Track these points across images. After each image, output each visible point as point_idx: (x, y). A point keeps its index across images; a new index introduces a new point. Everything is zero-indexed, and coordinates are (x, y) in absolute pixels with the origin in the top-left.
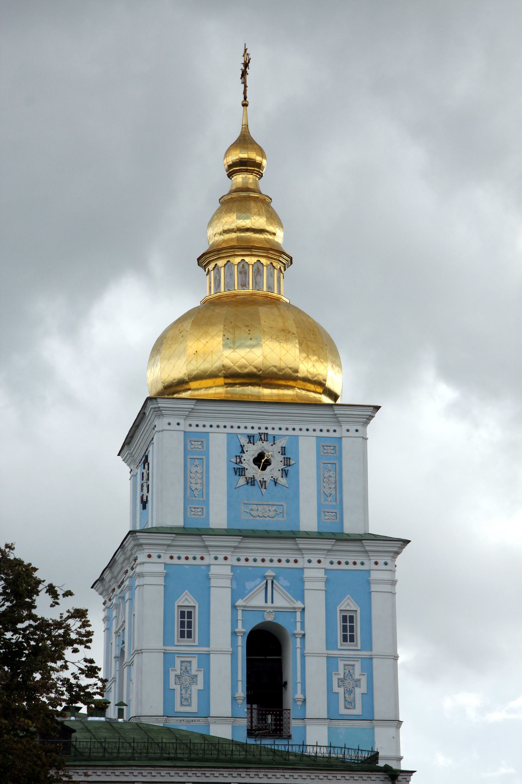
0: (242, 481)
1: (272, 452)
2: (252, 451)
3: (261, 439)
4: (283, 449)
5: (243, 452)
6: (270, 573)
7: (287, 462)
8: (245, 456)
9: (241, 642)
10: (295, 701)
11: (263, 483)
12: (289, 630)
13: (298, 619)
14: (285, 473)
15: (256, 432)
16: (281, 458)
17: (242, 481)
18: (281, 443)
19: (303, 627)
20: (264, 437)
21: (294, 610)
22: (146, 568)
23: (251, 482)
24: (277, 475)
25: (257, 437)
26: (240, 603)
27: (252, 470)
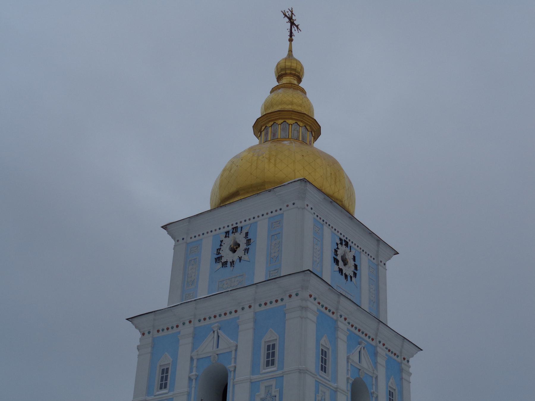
0: (336, 268)
1: (349, 257)
3: (345, 245)
4: (354, 257)
5: (338, 248)
7: (356, 266)
8: (339, 252)
11: (346, 276)
13: (374, 382)
14: (355, 274)
15: (342, 237)
16: (353, 263)
17: (336, 268)
20: (347, 244)
23: (341, 270)
24: (352, 275)
25: (344, 243)
27: (341, 263)
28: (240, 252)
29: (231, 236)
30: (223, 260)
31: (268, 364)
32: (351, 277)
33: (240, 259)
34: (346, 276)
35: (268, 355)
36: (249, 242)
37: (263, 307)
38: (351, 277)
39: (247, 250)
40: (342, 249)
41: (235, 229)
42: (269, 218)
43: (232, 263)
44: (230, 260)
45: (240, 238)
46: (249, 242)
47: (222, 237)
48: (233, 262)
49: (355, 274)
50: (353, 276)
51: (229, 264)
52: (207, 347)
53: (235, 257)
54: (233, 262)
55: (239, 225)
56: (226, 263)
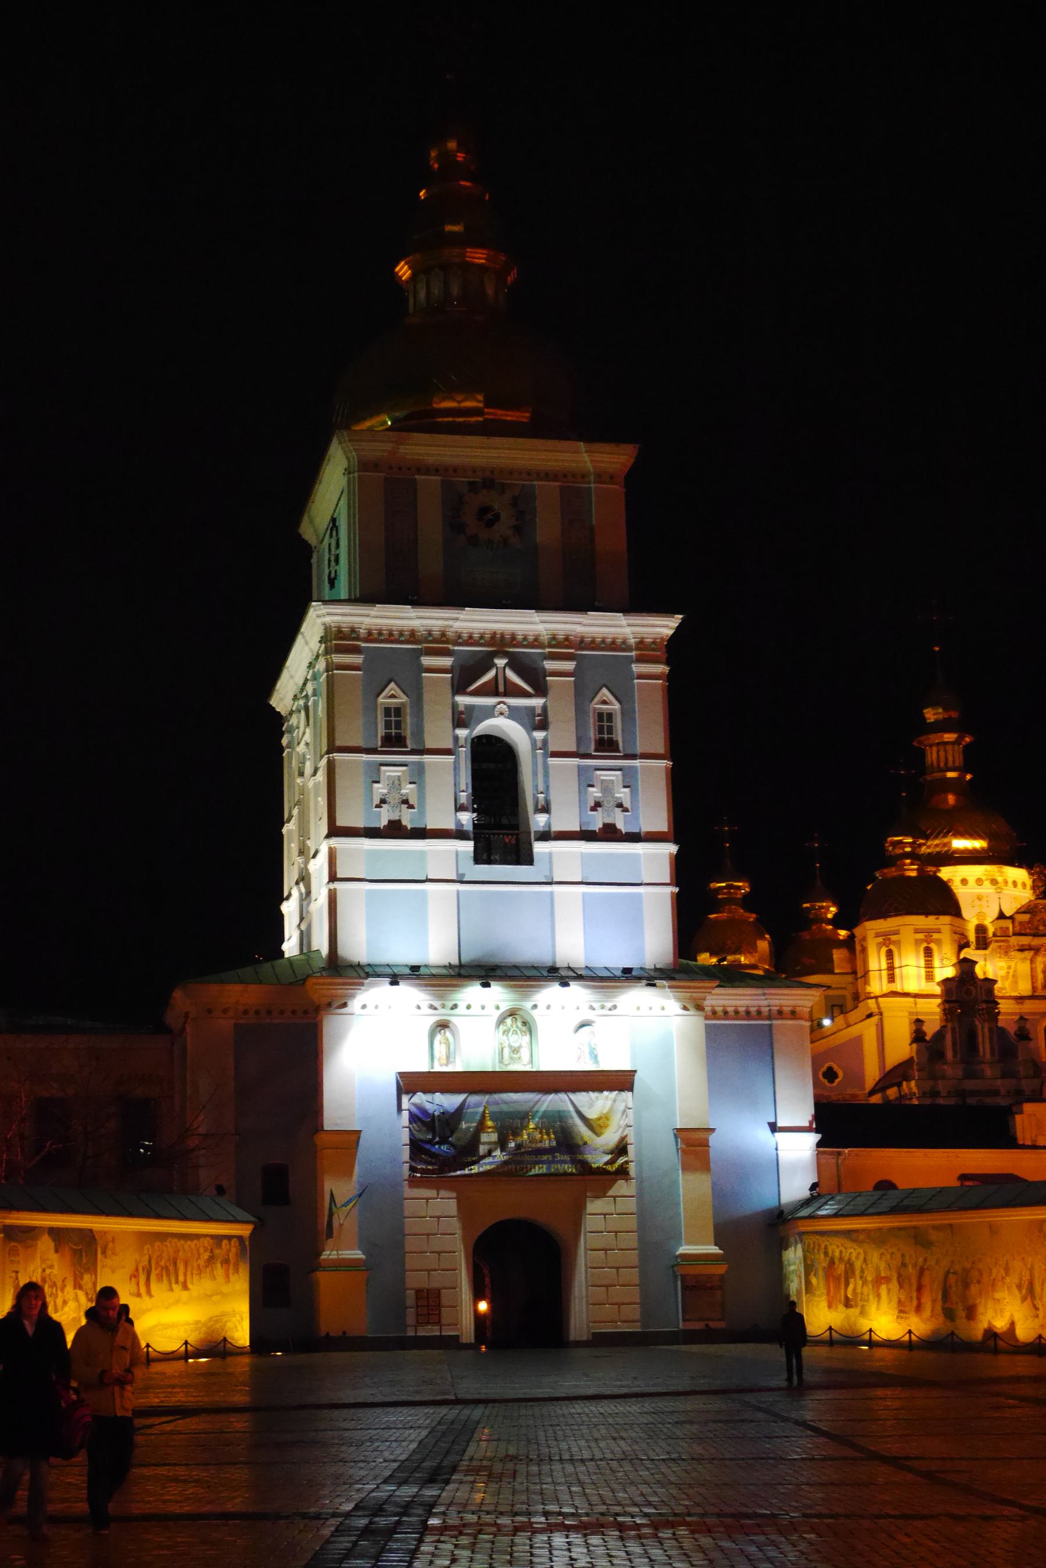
14: (518, 530)
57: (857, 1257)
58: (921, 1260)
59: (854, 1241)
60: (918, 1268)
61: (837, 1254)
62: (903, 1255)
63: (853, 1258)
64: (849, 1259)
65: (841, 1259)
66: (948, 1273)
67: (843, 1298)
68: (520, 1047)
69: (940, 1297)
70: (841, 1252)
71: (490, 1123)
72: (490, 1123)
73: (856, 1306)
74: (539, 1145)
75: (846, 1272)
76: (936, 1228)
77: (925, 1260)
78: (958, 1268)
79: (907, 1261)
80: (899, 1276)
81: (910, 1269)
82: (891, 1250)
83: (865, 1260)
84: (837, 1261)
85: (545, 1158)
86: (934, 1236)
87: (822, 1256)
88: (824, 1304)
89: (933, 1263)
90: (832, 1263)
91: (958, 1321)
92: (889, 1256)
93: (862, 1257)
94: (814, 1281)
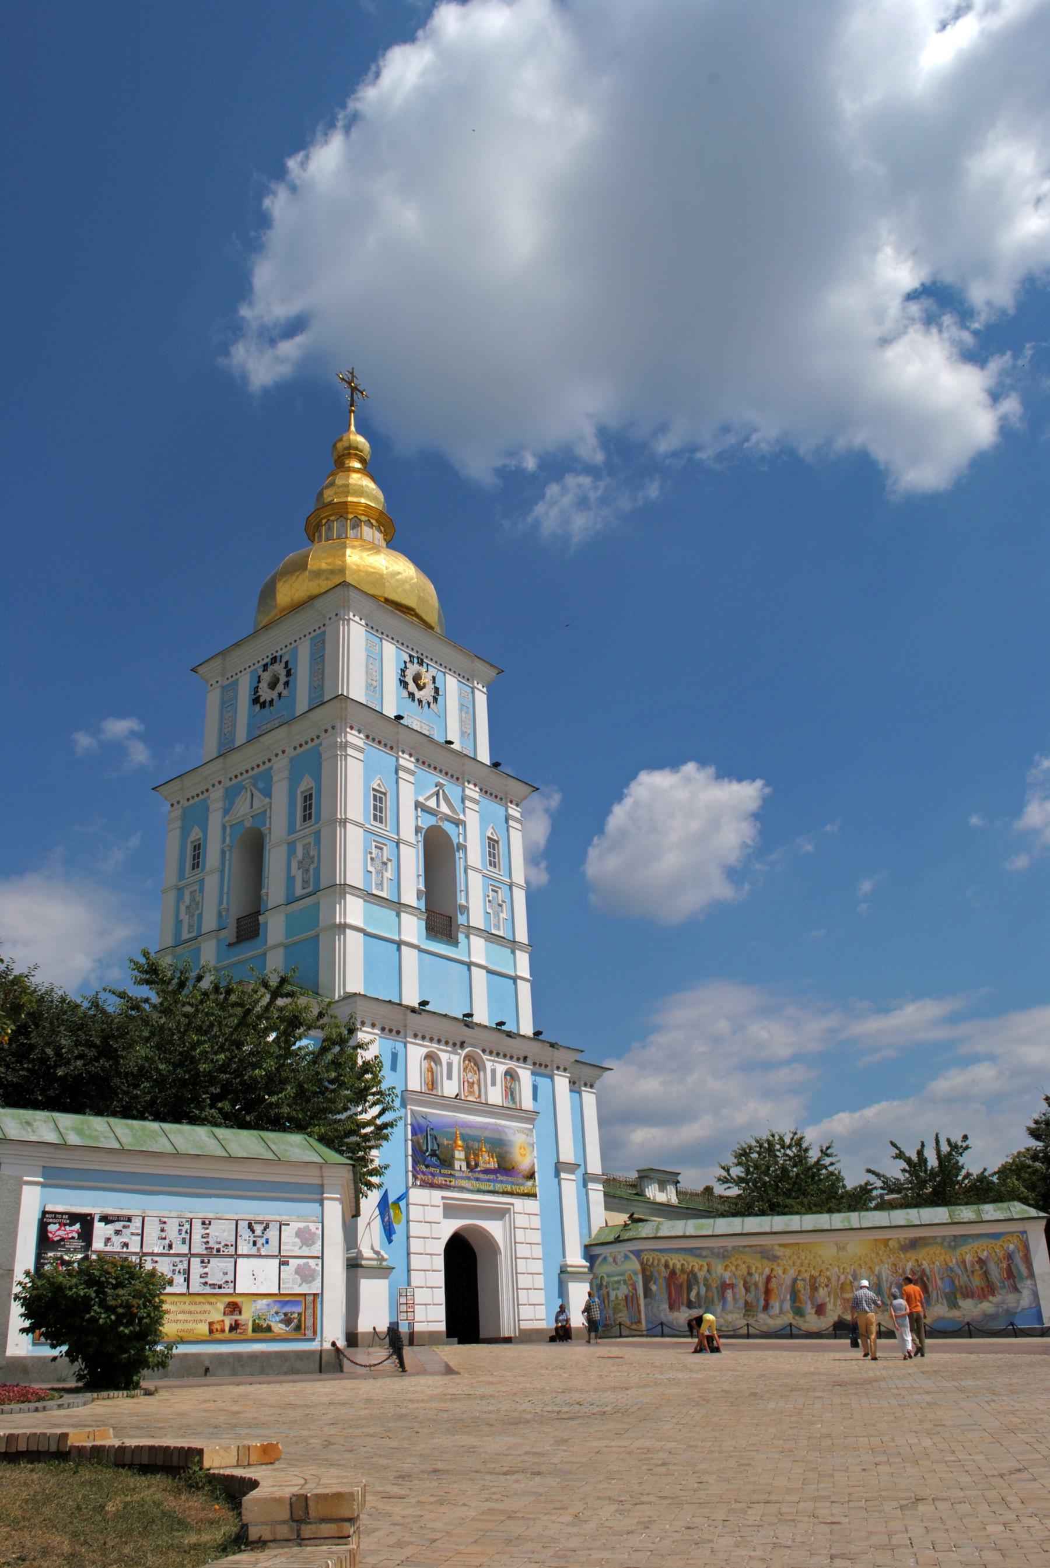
1: (426, 679)
2: (413, 669)
4: (434, 678)
6: (442, 781)
7: (437, 690)
8: (408, 672)
9: (421, 838)
10: (461, 907)
11: (420, 701)
12: (455, 841)
13: (461, 831)
17: (405, 694)
18: (433, 671)
19: (465, 840)
20: (421, 663)
21: (458, 823)
22: (351, 738)
23: (411, 695)
24: (431, 700)
25: (416, 661)
26: (421, 799)
27: (412, 687)
28: (280, 687)
29: (270, 668)
30: (262, 700)
31: (305, 820)
32: (429, 704)
33: (280, 695)
34: (420, 701)
35: (305, 807)
36: (289, 674)
37: (299, 750)
38: (429, 704)
39: (287, 684)
40: (413, 669)
41: (274, 660)
42: (312, 639)
43: (271, 702)
44: (269, 699)
45: (279, 668)
46: (289, 674)
47: (260, 672)
48: (272, 700)
49: (435, 700)
50: (431, 700)
51: (267, 704)
52: (242, 808)
53: (274, 695)
54: (272, 700)
55: (278, 654)
56: (265, 702)
57: (701, 1268)
58: (767, 1271)
59: (699, 1256)
60: (764, 1277)
61: (679, 1266)
62: (749, 1267)
63: (696, 1270)
64: (692, 1271)
65: (683, 1270)
66: (795, 1281)
67: (685, 1301)
68: (473, 1083)
69: (788, 1297)
70: (682, 1265)
71: (460, 1143)
72: (460, 1143)
73: (700, 1307)
74: (488, 1166)
75: (688, 1281)
76: (781, 1245)
77: (772, 1270)
78: (806, 1276)
79: (753, 1270)
80: (745, 1283)
81: (757, 1276)
82: (735, 1263)
83: (708, 1271)
84: (678, 1272)
85: (492, 1177)
86: (779, 1252)
87: (663, 1269)
88: (666, 1306)
89: (780, 1272)
90: (673, 1273)
91: (807, 1317)
92: (733, 1268)
93: (706, 1268)
94: (654, 1288)
